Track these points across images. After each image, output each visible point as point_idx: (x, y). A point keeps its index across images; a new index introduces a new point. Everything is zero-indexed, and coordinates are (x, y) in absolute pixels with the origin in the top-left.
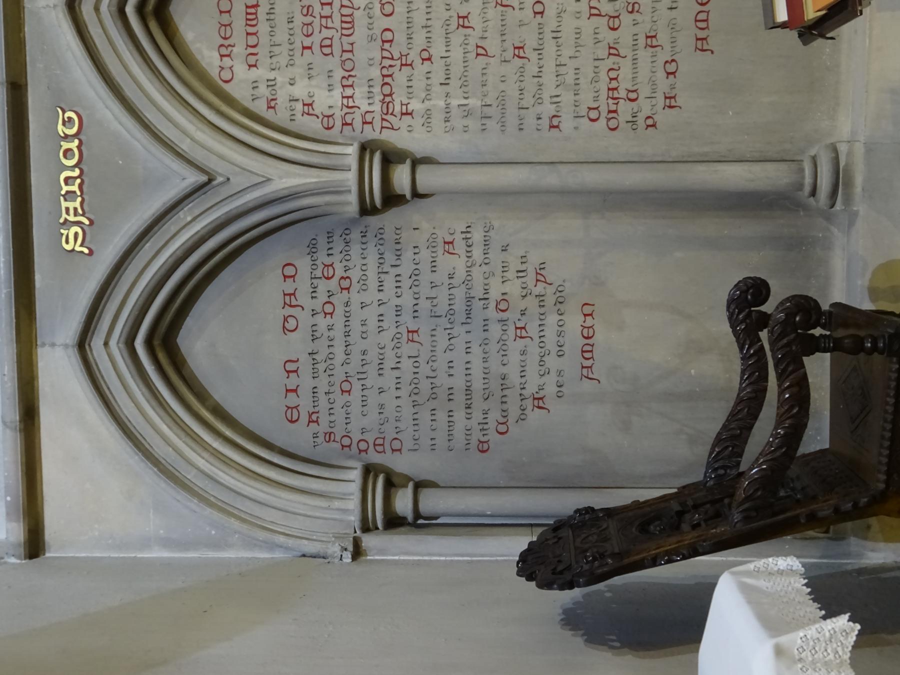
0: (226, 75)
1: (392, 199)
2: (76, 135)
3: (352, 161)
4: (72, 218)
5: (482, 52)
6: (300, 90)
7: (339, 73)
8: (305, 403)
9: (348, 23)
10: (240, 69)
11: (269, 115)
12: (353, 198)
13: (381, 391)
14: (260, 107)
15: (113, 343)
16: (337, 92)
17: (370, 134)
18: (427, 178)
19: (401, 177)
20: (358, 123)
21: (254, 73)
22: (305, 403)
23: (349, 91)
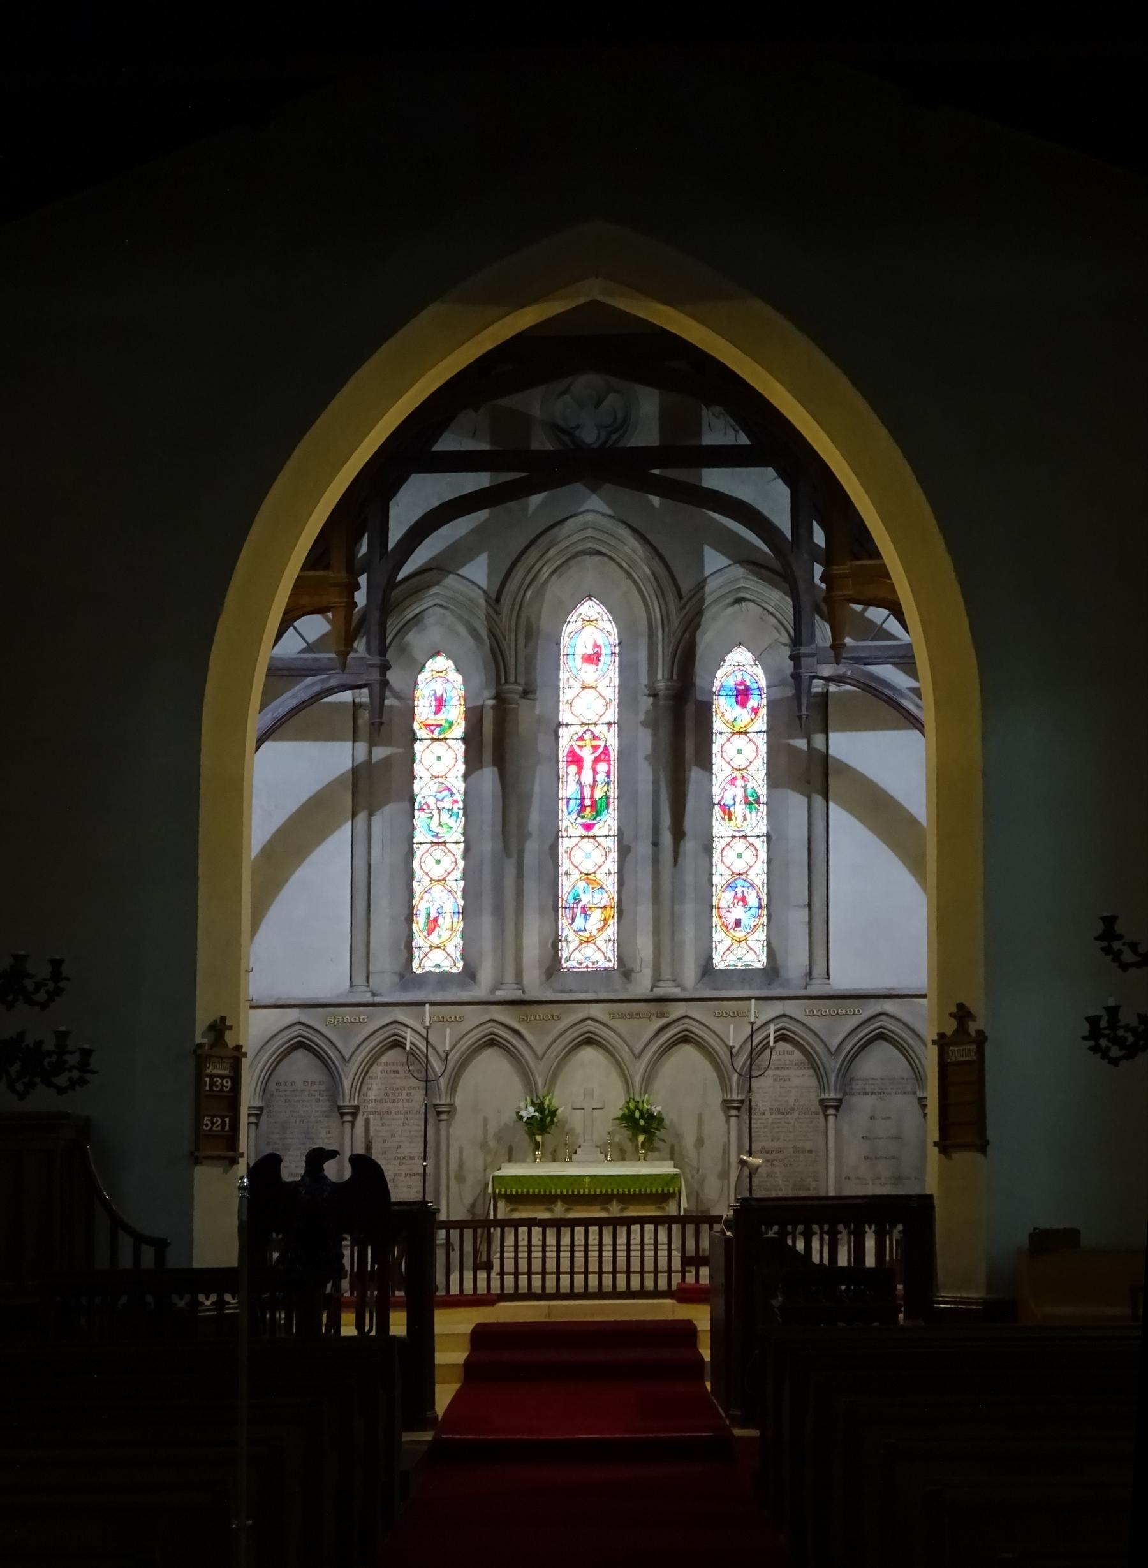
0: (379, 1064)
1: (342, 1115)
2: (360, 1022)
3: (352, 1103)
4: (336, 1020)
5: (384, 1141)
6: (375, 1087)
7: (379, 1098)
8: (282, 1088)
9: (393, 1101)
10: (380, 1068)
11: (367, 1077)
12: (342, 1104)
13: (285, 1112)
14: (369, 1074)
15: (301, 1032)
16: (374, 1098)
17: (362, 1109)
18: (348, 1126)
19: (348, 1118)
20: (364, 1104)
21: (379, 1073)
22: (282, 1088)
23: (374, 1101)
